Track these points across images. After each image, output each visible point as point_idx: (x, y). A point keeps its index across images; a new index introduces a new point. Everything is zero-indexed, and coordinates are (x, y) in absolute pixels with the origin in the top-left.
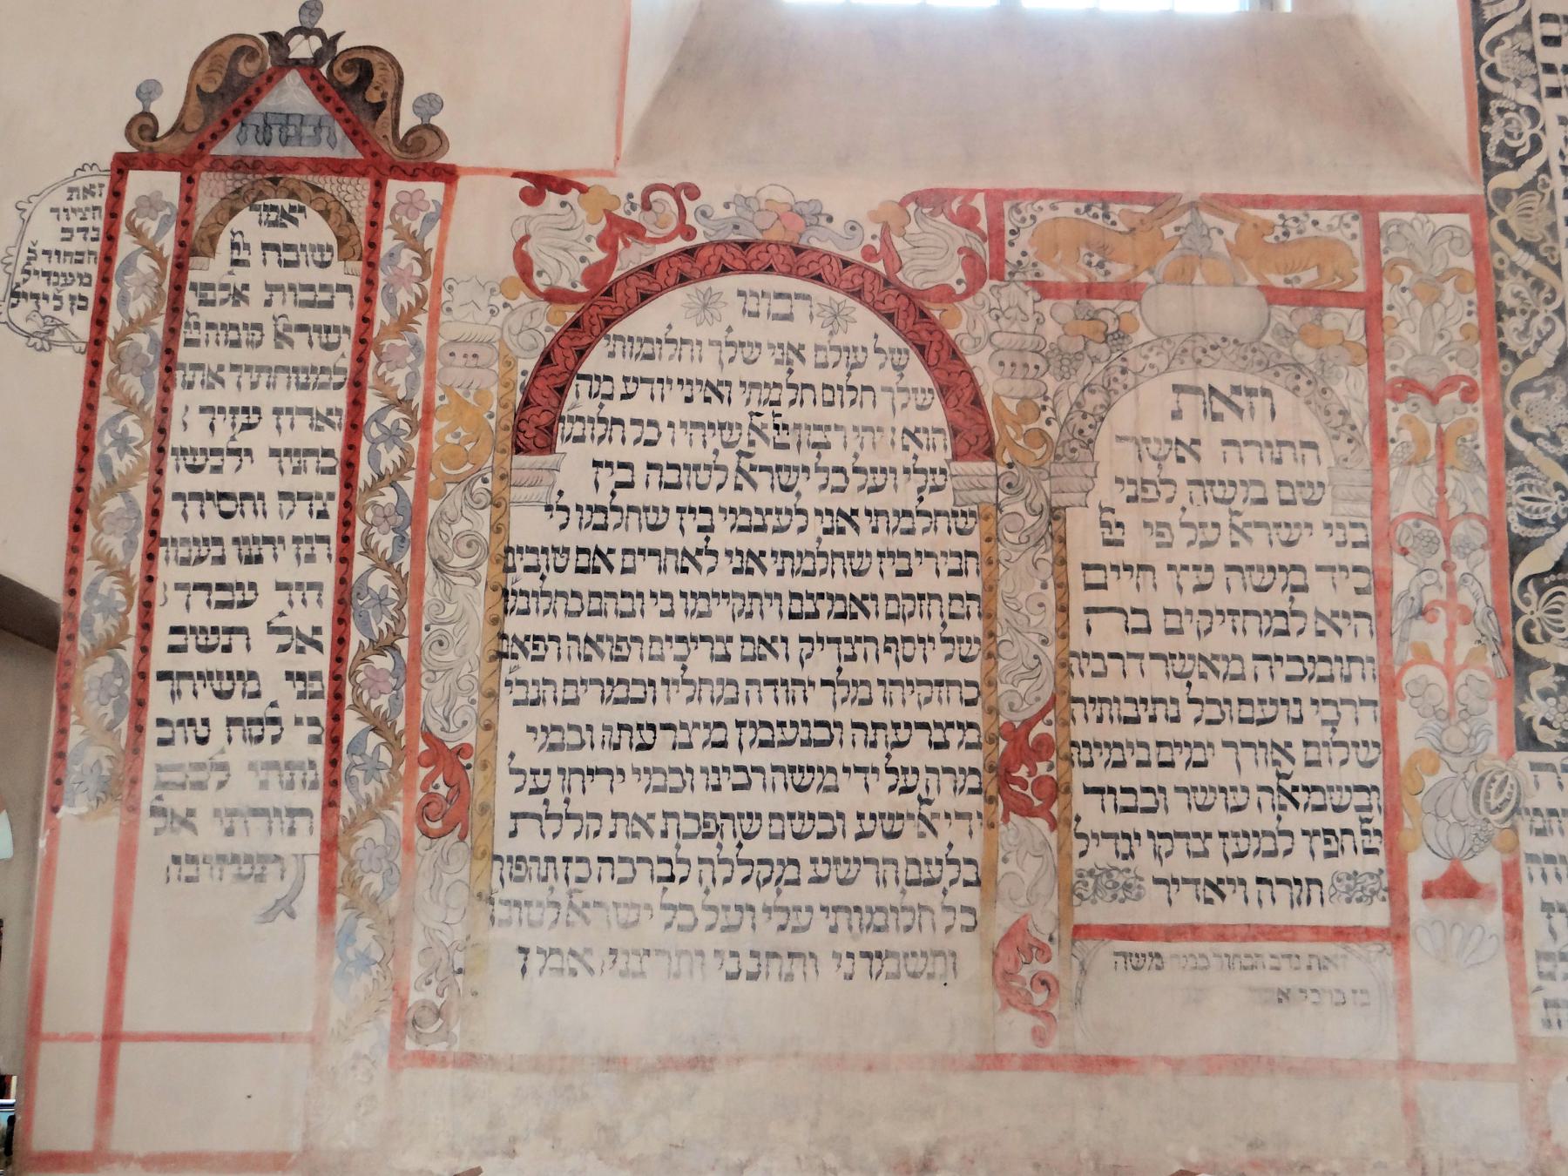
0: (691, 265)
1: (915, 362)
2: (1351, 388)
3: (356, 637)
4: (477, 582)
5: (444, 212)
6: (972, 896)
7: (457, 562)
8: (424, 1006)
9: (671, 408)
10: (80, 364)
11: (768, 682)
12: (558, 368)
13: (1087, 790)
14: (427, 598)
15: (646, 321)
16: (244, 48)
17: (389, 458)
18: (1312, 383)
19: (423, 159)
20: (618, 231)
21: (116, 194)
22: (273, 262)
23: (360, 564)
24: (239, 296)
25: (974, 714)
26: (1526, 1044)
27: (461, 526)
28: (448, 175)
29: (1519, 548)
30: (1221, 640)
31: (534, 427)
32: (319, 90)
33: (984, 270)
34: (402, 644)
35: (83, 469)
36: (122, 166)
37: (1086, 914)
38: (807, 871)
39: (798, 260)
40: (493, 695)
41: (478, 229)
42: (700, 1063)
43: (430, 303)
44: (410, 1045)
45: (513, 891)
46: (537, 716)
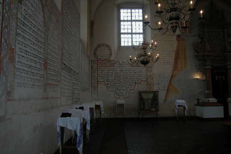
1: (42, 12)
3: (4, 24)
4: (15, 22)
6: (43, 79)
7: (13, 17)
8: (9, 91)
11: (34, 49)
13: (48, 68)
14: (11, 22)
23: (5, 11)
25: (43, 57)
26: (60, 95)
27: (14, 11)
34: (8, 28)
37: (49, 82)
38: (35, 74)
40: (16, 41)
42: (28, 100)
44: (8, 98)
45: (17, 73)
46: (20, 47)
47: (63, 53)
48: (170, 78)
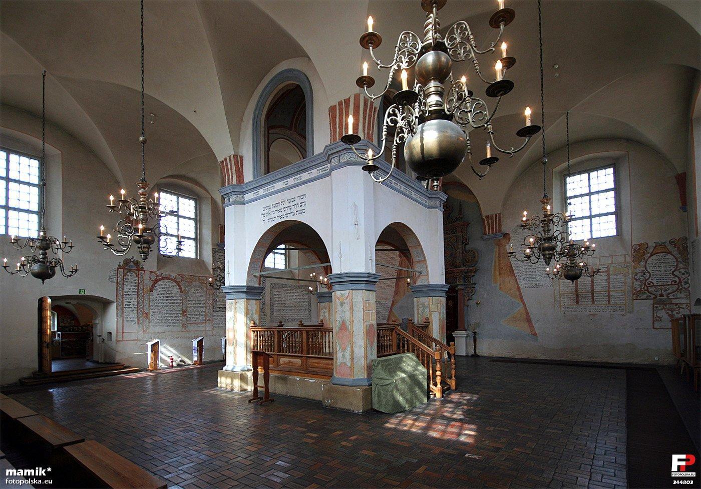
0: (162, 279)
2: (205, 289)
5: (144, 274)
9: (161, 289)
10: (116, 284)
12: (153, 286)
15: (159, 283)
16: (127, 260)
17: (141, 292)
18: (202, 289)
19: (142, 269)
20: (157, 276)
21: (118, 271)
22: (130, 276)
24: (129, 279)
28: (144, 271)
29: (214, 299)
30: (197, 305)
31: (151, 290)
32: (134, 264)
33: (182, 280)
35: (117, 292)
36: (118, 269)
39: (169, 279)
41: (147, 275)
43: (143, 281)
47: (216, 300)
48: (391, 304)
